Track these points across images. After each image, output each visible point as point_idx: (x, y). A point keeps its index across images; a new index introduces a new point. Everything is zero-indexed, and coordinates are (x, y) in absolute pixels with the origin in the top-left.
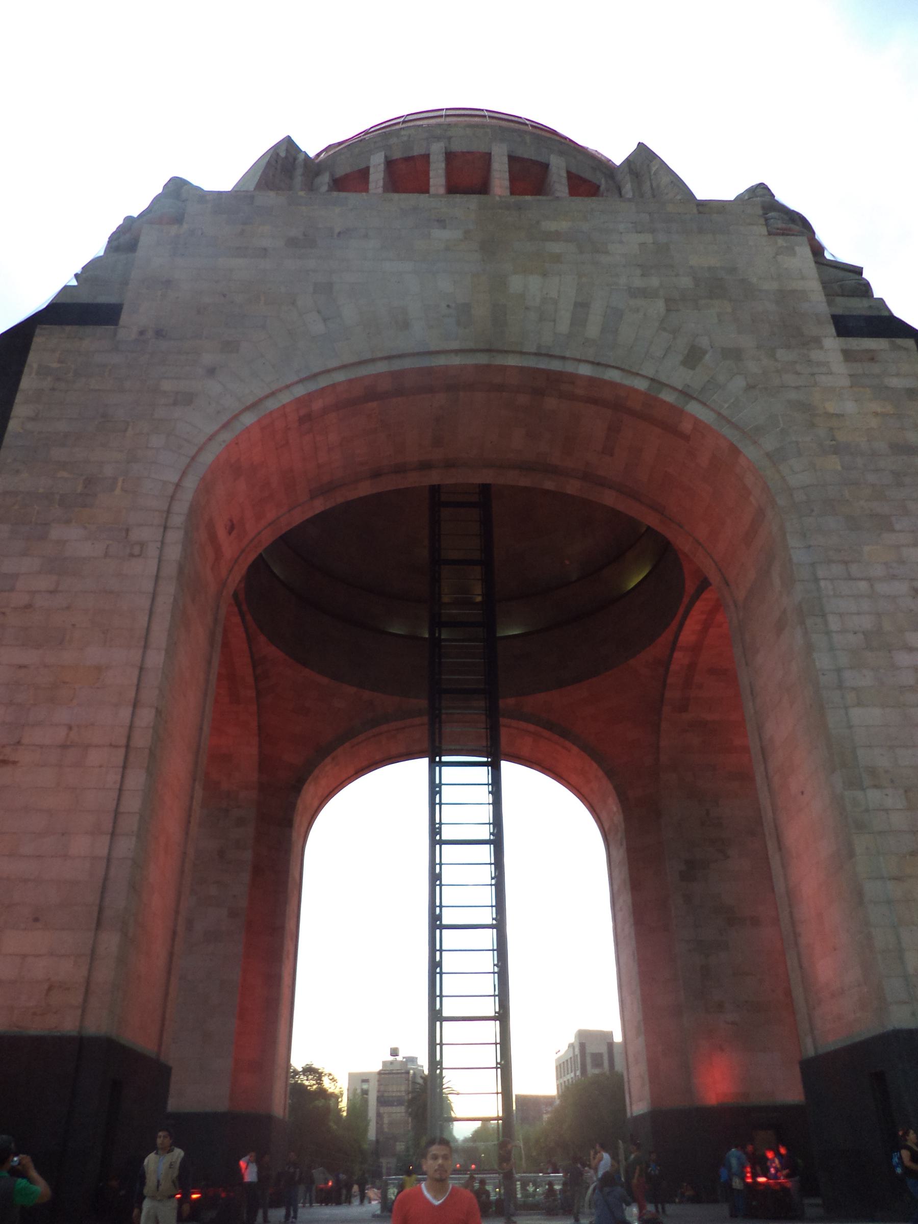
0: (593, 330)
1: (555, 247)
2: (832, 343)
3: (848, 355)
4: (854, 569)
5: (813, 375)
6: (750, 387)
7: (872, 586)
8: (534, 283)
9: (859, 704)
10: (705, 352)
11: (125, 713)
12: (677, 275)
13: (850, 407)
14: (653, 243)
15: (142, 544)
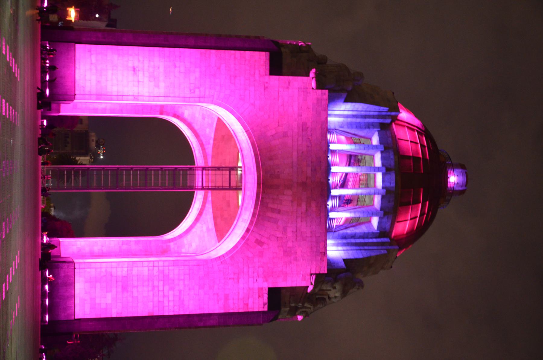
0: (269, 214)
1: (304, 205)
2: (266, 286)
3: (260, 289)
4: (187, 276)
5: (253, 277)
6: (248, 257)
7: (182, 280)
8: (290, 198)
9: (149, 270)
10: (261, 246)
11: (147, 94)
12: (293, 242)
13: (241, 286)
14: (306, 236)
15: (194, 92)
